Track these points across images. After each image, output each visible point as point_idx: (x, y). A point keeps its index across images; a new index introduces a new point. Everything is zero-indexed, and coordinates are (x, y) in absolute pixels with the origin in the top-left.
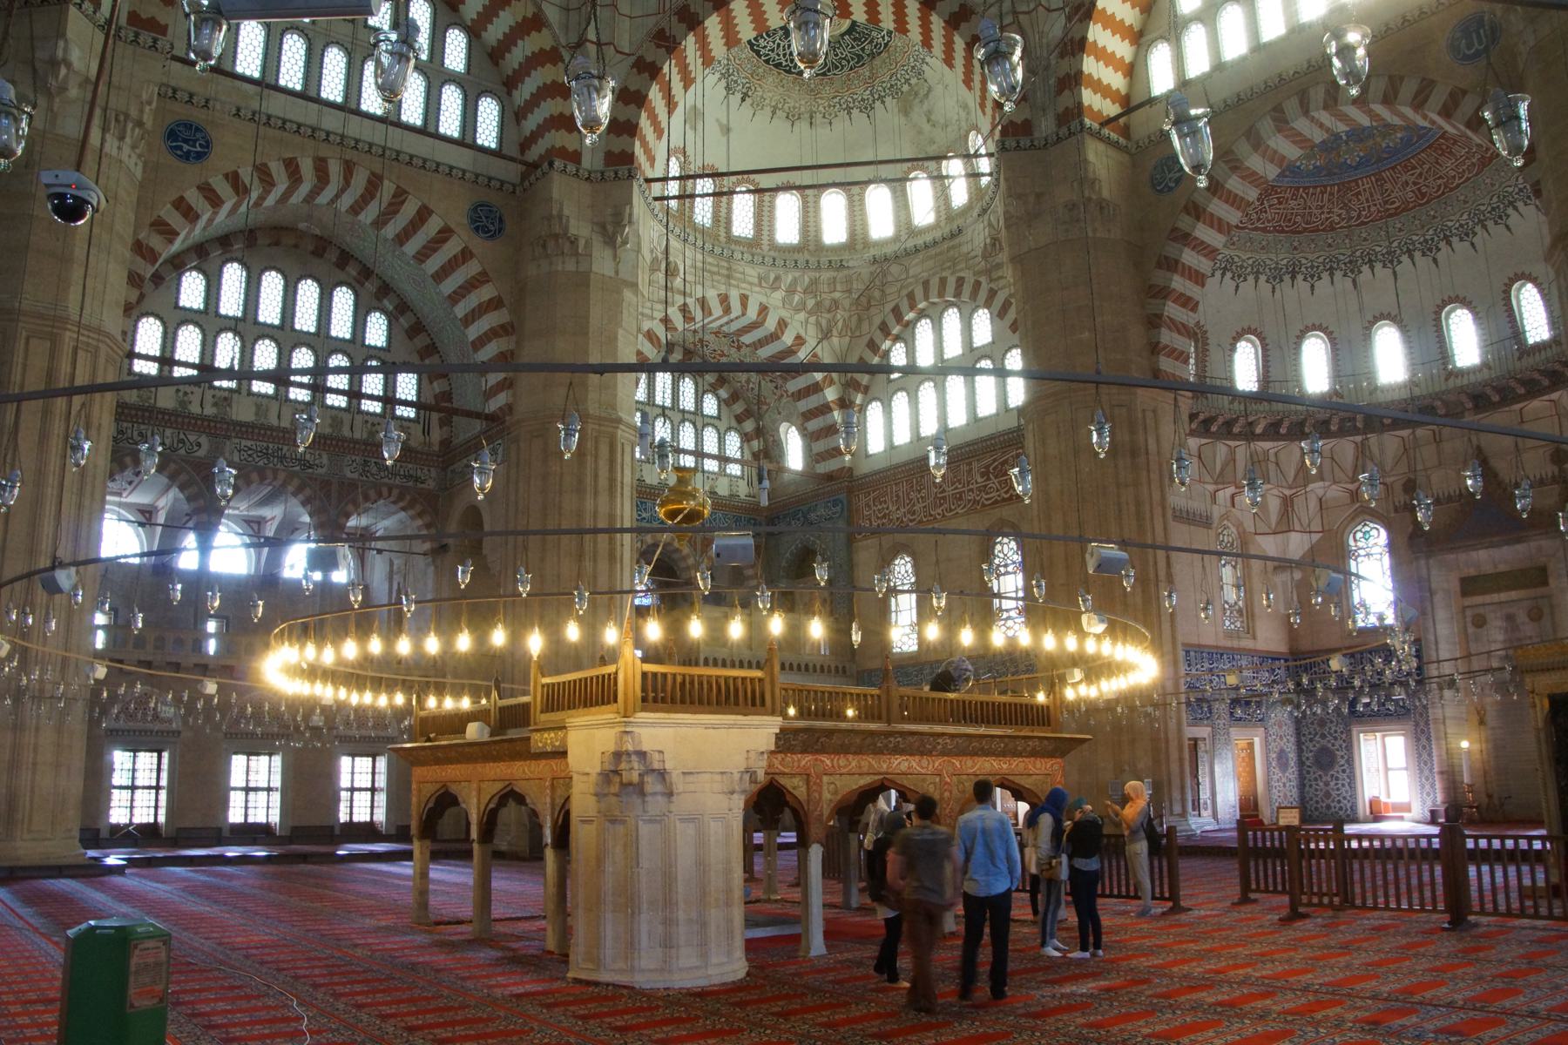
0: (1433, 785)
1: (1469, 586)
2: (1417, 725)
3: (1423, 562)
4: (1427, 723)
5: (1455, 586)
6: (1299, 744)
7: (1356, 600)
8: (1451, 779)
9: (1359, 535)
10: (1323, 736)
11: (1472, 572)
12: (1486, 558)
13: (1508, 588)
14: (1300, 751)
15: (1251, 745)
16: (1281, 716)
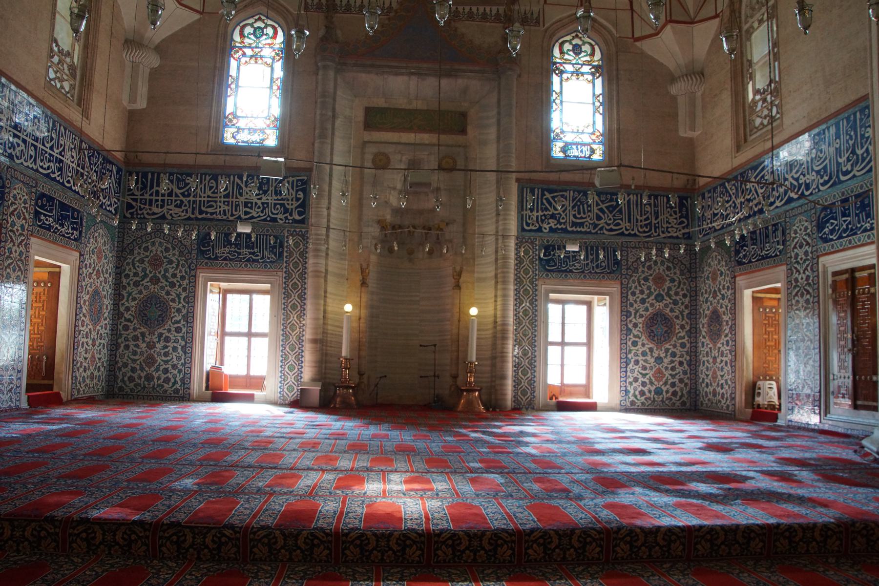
0: (299, 357)
1: (376, 118)
2: (288, 276)
3: (331, 74)
4: (303, 276)
5: (360, 116)
6: (118, 287)
7: (229, 109)
8: (324, 345)
9: (248, 30)
10: (155, 281)
11: (381, 103)
12: (403, 88)
13: (421, 129)
14: (118, 297)
15: (55, 276)
16: (99, 241)
